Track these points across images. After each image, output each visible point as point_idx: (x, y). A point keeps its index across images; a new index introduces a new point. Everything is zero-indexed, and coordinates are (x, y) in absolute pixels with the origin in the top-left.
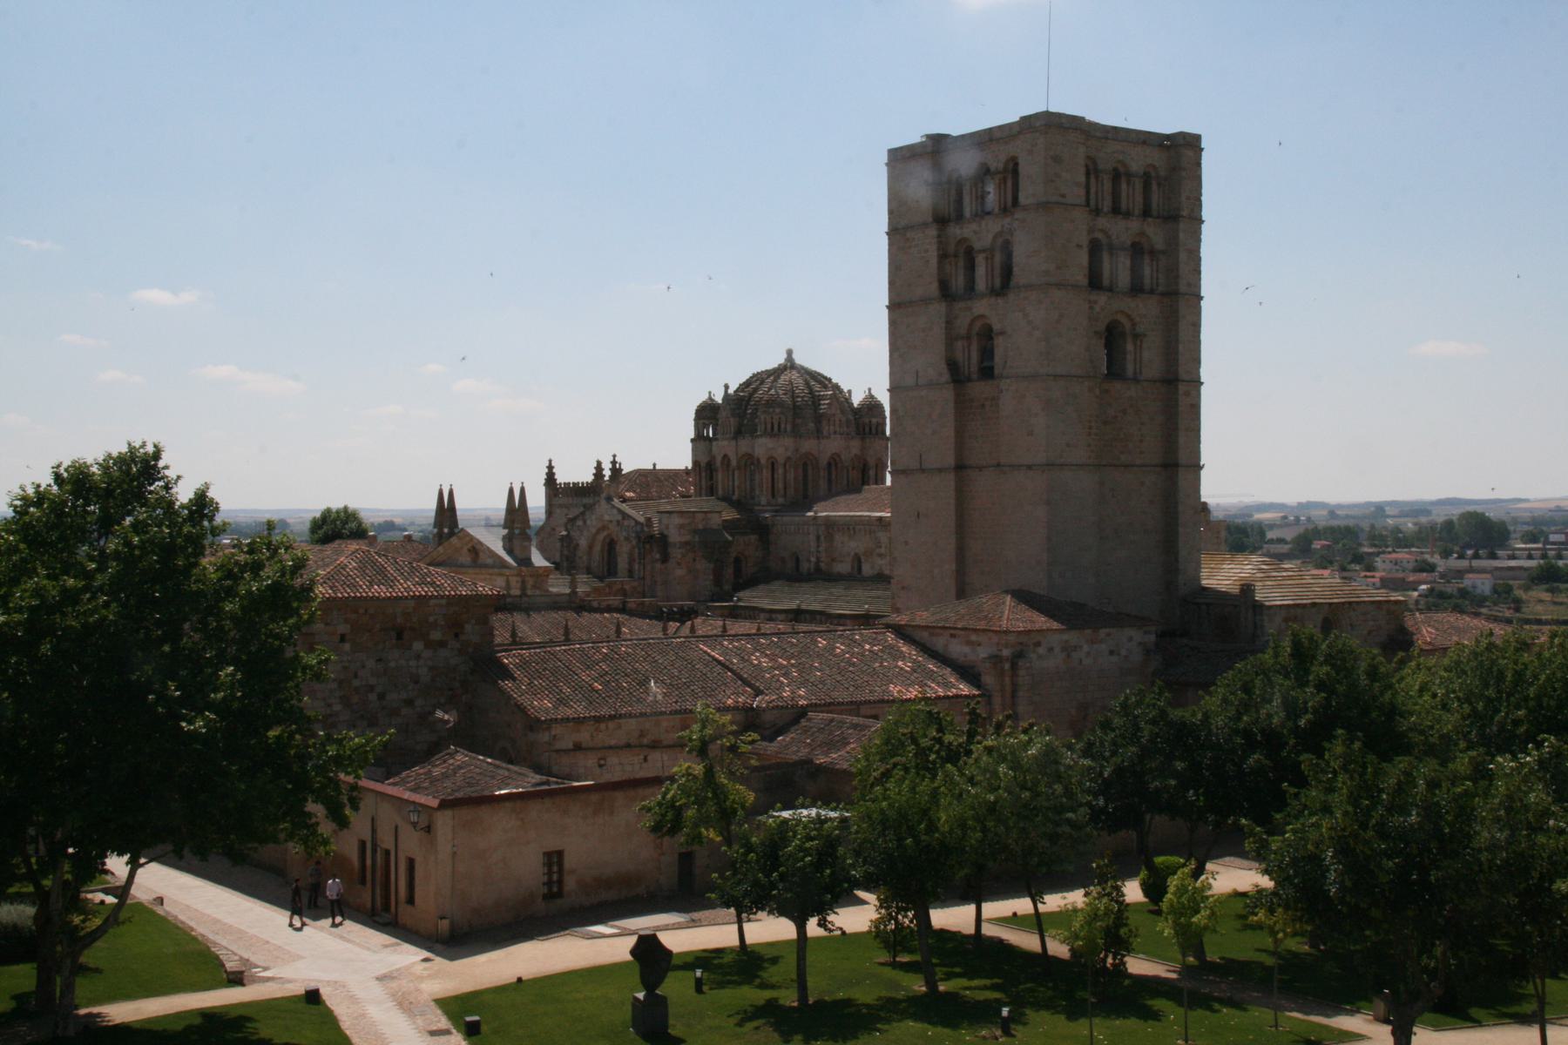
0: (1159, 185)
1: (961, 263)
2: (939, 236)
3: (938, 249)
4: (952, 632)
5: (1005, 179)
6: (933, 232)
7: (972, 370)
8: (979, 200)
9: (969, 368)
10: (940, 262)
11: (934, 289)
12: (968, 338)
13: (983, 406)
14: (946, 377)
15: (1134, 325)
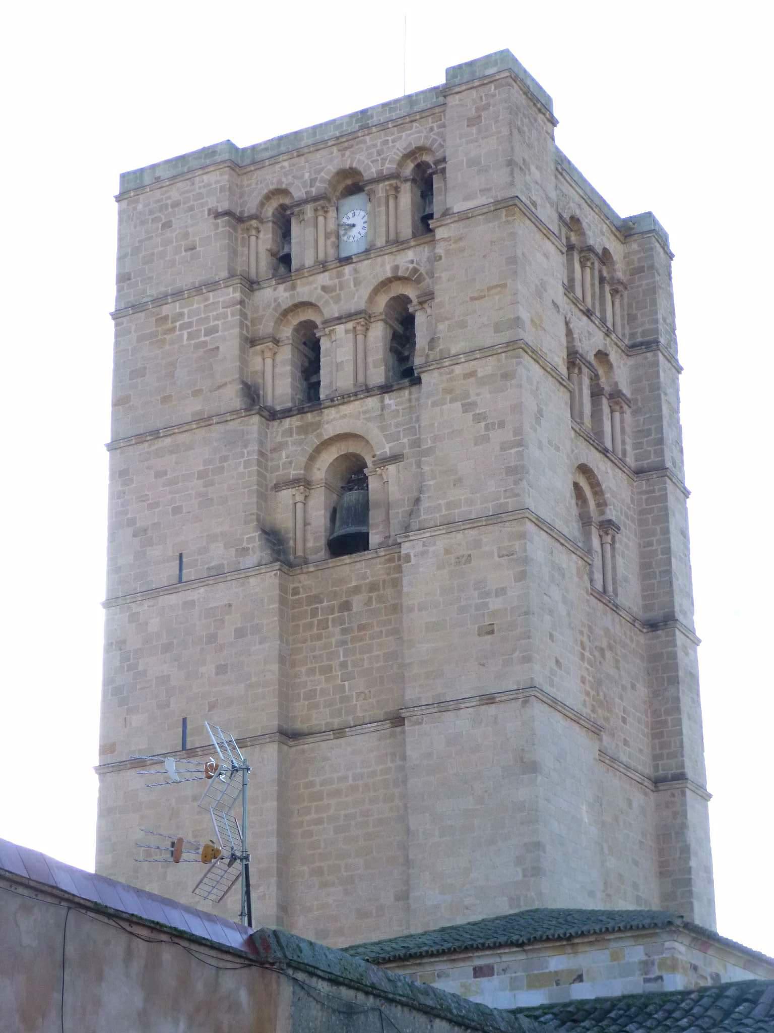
0: (615, 292)
1: (286, 353)
2: (242, 302)
3: (242, 325)
4: (482, 959)
5: (397, 189)
6: (233, 294)
7: (310, 544)
8: (333, 239)
9: (305, 541)
10: (242, 350)
11: (232, 397)
12: (304, 483)
13: (346, 606)
14: (257, 552)
15: (602, 505)
